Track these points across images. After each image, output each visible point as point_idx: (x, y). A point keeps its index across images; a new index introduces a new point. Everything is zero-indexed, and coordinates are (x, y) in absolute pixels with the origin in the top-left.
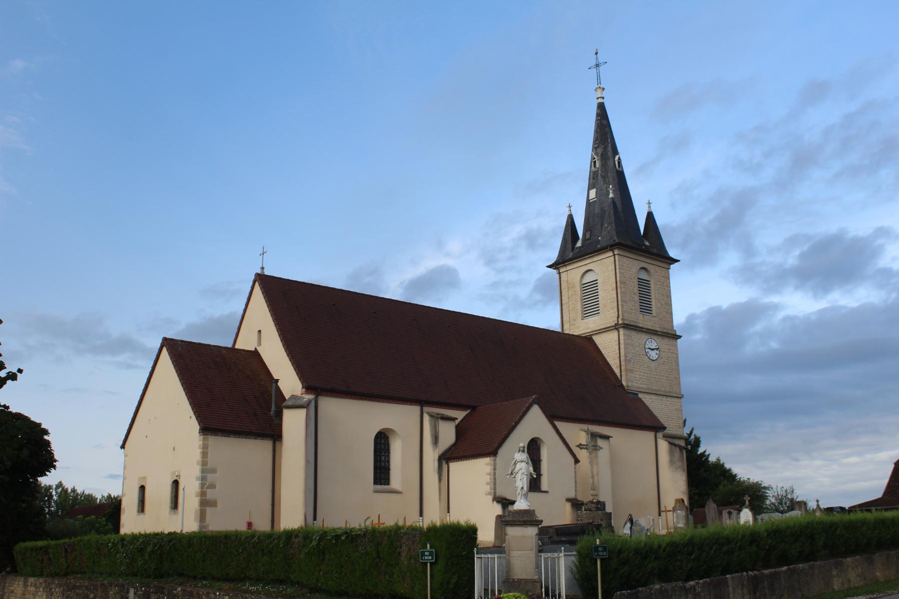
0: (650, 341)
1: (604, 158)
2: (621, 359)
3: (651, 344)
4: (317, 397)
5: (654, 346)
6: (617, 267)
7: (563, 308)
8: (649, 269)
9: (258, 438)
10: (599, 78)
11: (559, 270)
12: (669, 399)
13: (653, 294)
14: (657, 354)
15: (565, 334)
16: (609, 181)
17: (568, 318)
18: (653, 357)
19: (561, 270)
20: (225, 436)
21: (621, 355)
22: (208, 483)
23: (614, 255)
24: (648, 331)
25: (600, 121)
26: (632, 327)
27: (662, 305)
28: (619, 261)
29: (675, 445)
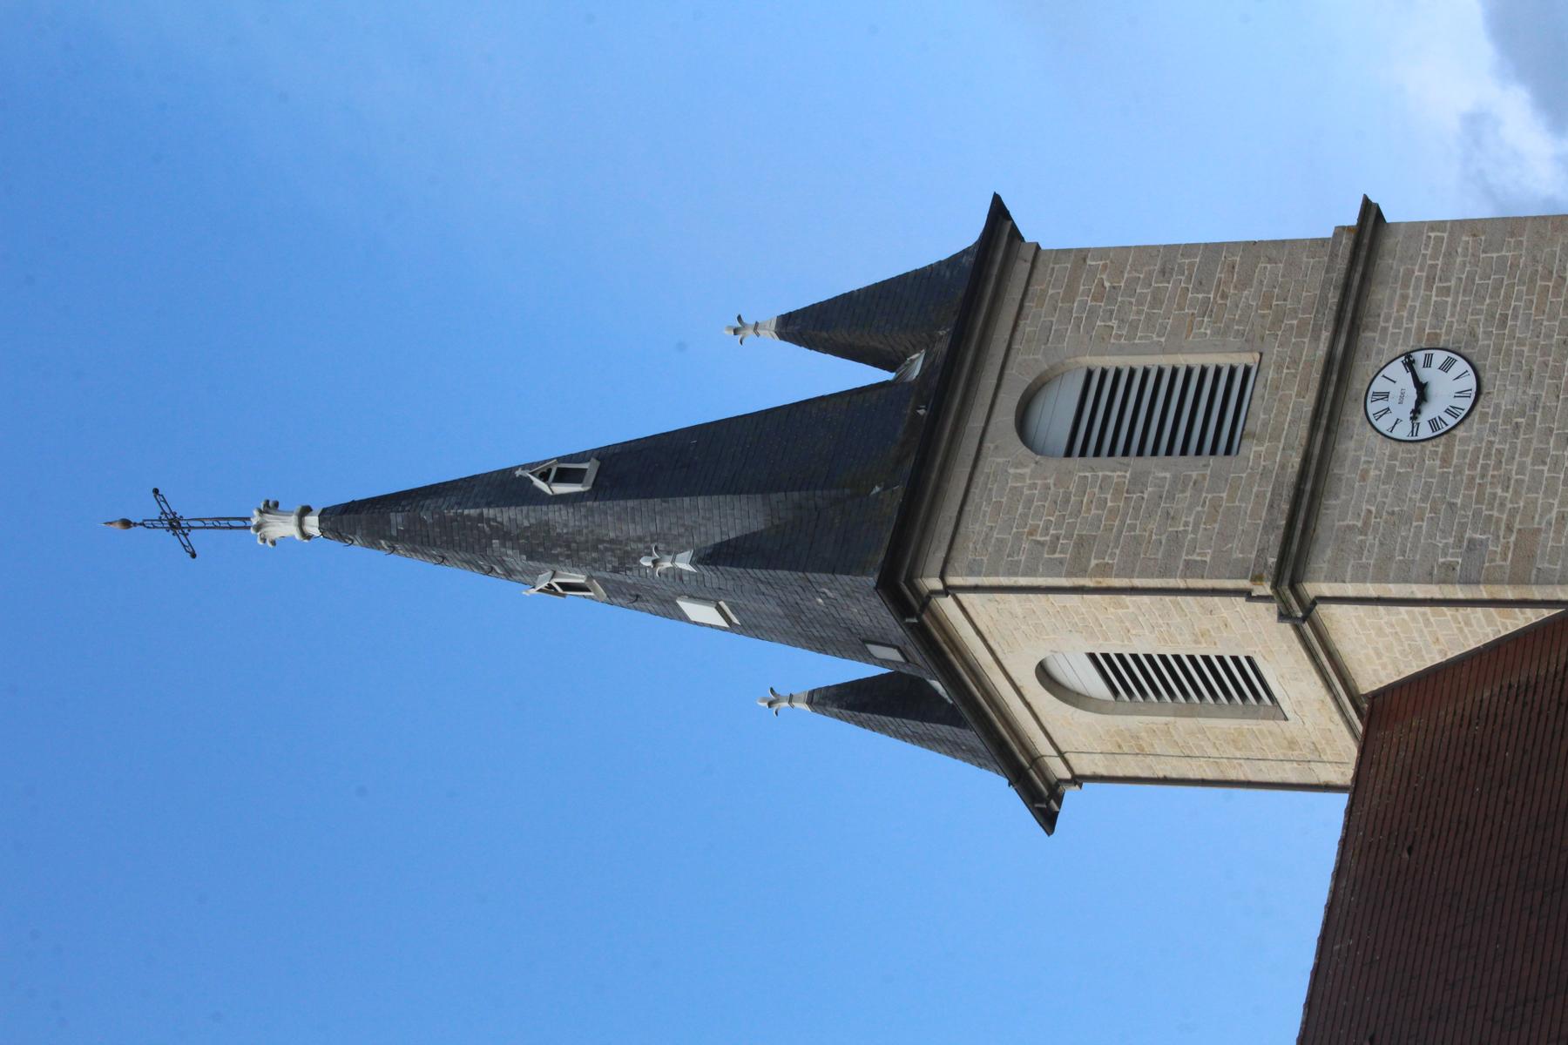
0: (1381, 405)
3: (1392, 402)
5: (1397, 381)
7: (1242, 778)
10: (223, 523)
11: (1061, 781)
13: (1153, 361)
14: (1445, 367)
16: (640, 539)
17: (1288, 766)
18: (1460, 394)
19: (1059, 770)
23: (948, 590)
24: (1324, 422)
25: (397, 540)
26: (1300, 525)
27: (1205, 308)
28: (972, 573)
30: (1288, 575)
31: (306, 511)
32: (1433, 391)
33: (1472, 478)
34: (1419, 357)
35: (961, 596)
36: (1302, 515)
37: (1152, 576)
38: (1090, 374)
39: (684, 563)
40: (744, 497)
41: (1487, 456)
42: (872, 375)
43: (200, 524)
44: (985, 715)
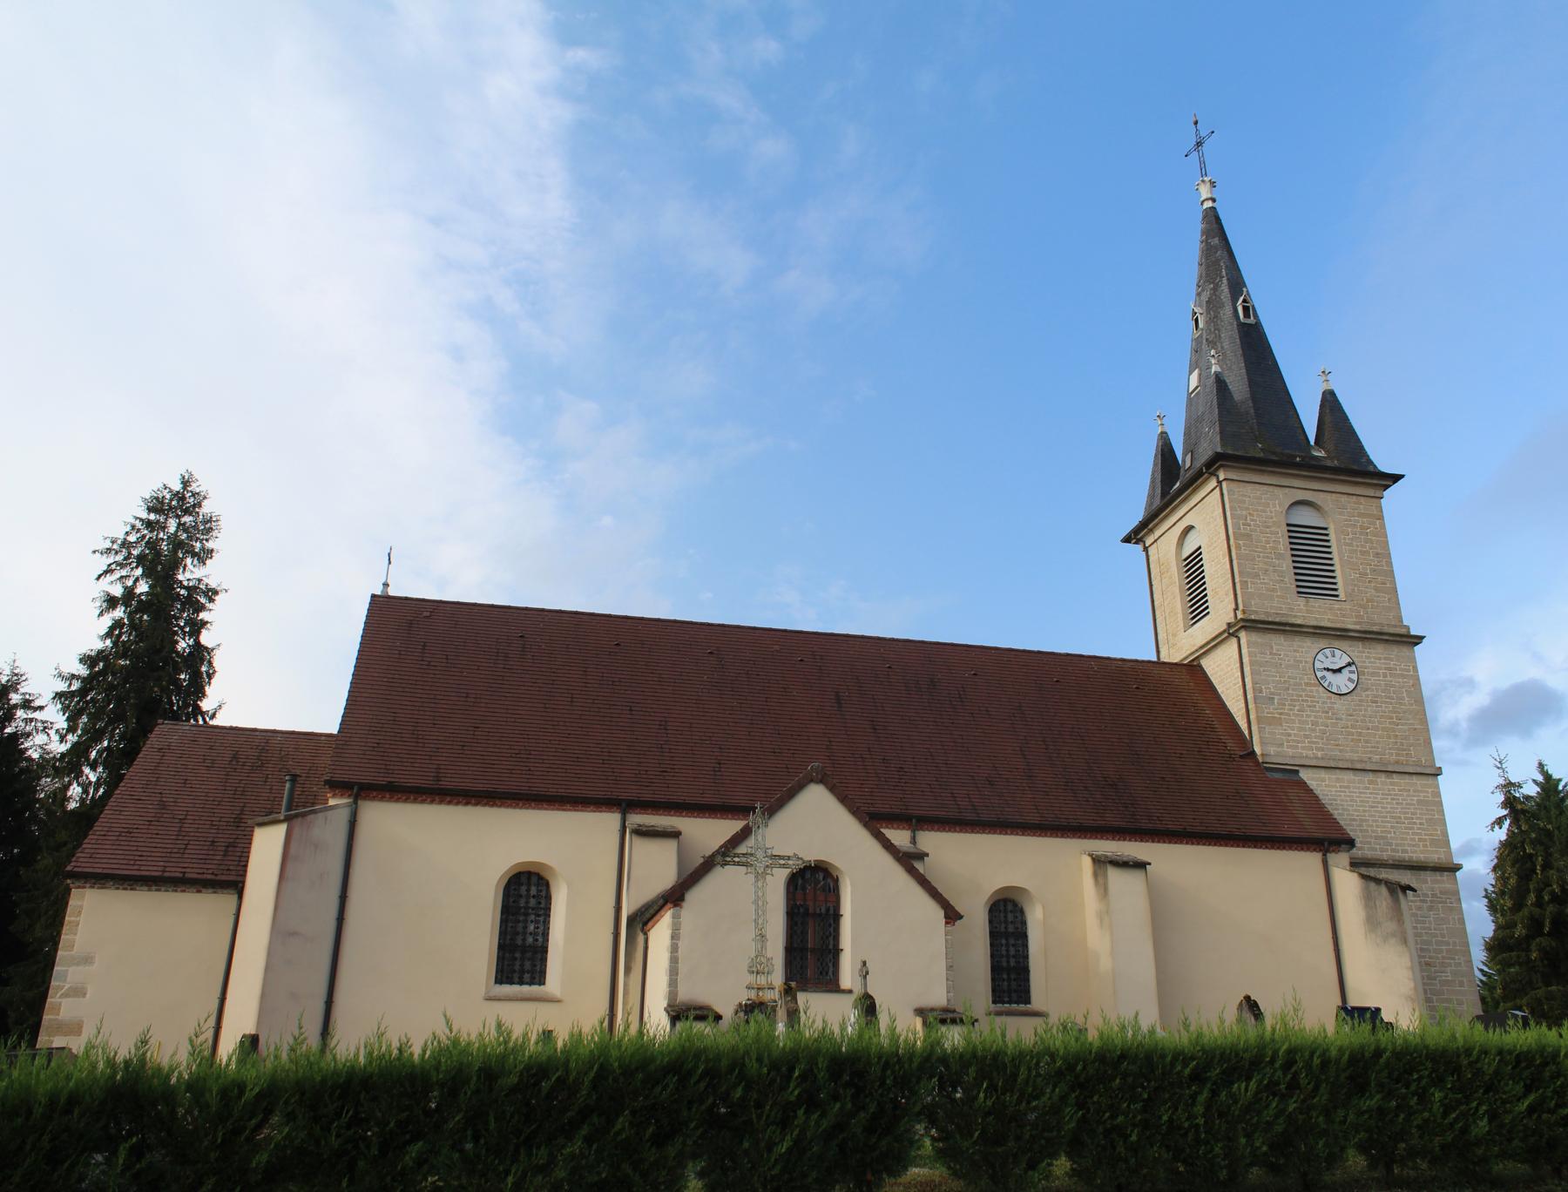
0: (1329, 654)
1: (1212, 305)
2: (1248, 697)
4: (355, 802)
6: (1227, 506)
7: (1157, 617)
8: (1319, 503)
9: (204, 890)
10: (1203, 166)
11: (1144, 542)
12: (1396, 778)
14: (1350, 680)
15: (1164, 663)
16: (1222, 347)
18: (1338, 687)
20: (125, 889)
21: (1247, 687)
22: (67, 986)
23: (1220, 483)
27: (1363, 574)
29: (1378, 881)
30: (1248, 624)
31: (1214, 200)
32: (1338, 675)
33: (1301, 696)
34: (1353, 668)
35: (1218, 488)
36: (1275, 627)
37: (1239, 567)
38: (1326, 529)
39: (1214, 369)
40: (1248, 389)
41: (1312, 701)
42: (1312, 434)
43: (1201, 155)
44: (1168, 507)
